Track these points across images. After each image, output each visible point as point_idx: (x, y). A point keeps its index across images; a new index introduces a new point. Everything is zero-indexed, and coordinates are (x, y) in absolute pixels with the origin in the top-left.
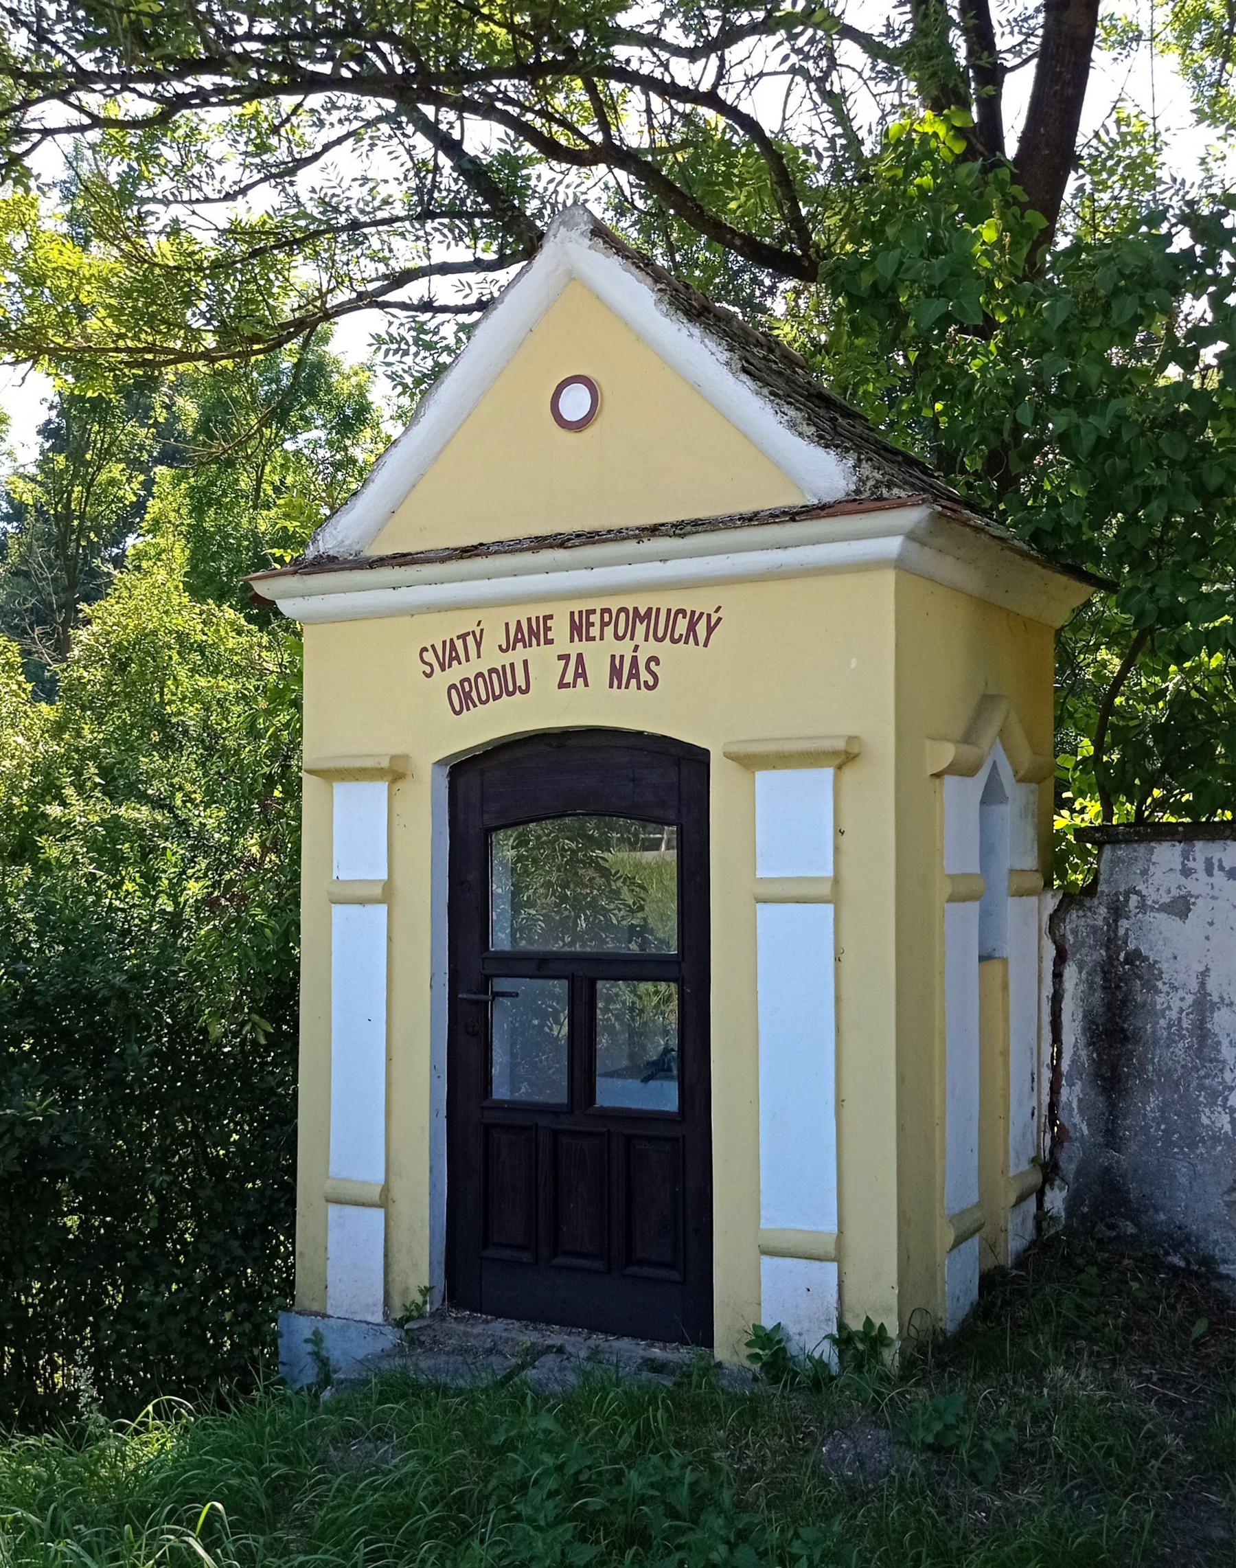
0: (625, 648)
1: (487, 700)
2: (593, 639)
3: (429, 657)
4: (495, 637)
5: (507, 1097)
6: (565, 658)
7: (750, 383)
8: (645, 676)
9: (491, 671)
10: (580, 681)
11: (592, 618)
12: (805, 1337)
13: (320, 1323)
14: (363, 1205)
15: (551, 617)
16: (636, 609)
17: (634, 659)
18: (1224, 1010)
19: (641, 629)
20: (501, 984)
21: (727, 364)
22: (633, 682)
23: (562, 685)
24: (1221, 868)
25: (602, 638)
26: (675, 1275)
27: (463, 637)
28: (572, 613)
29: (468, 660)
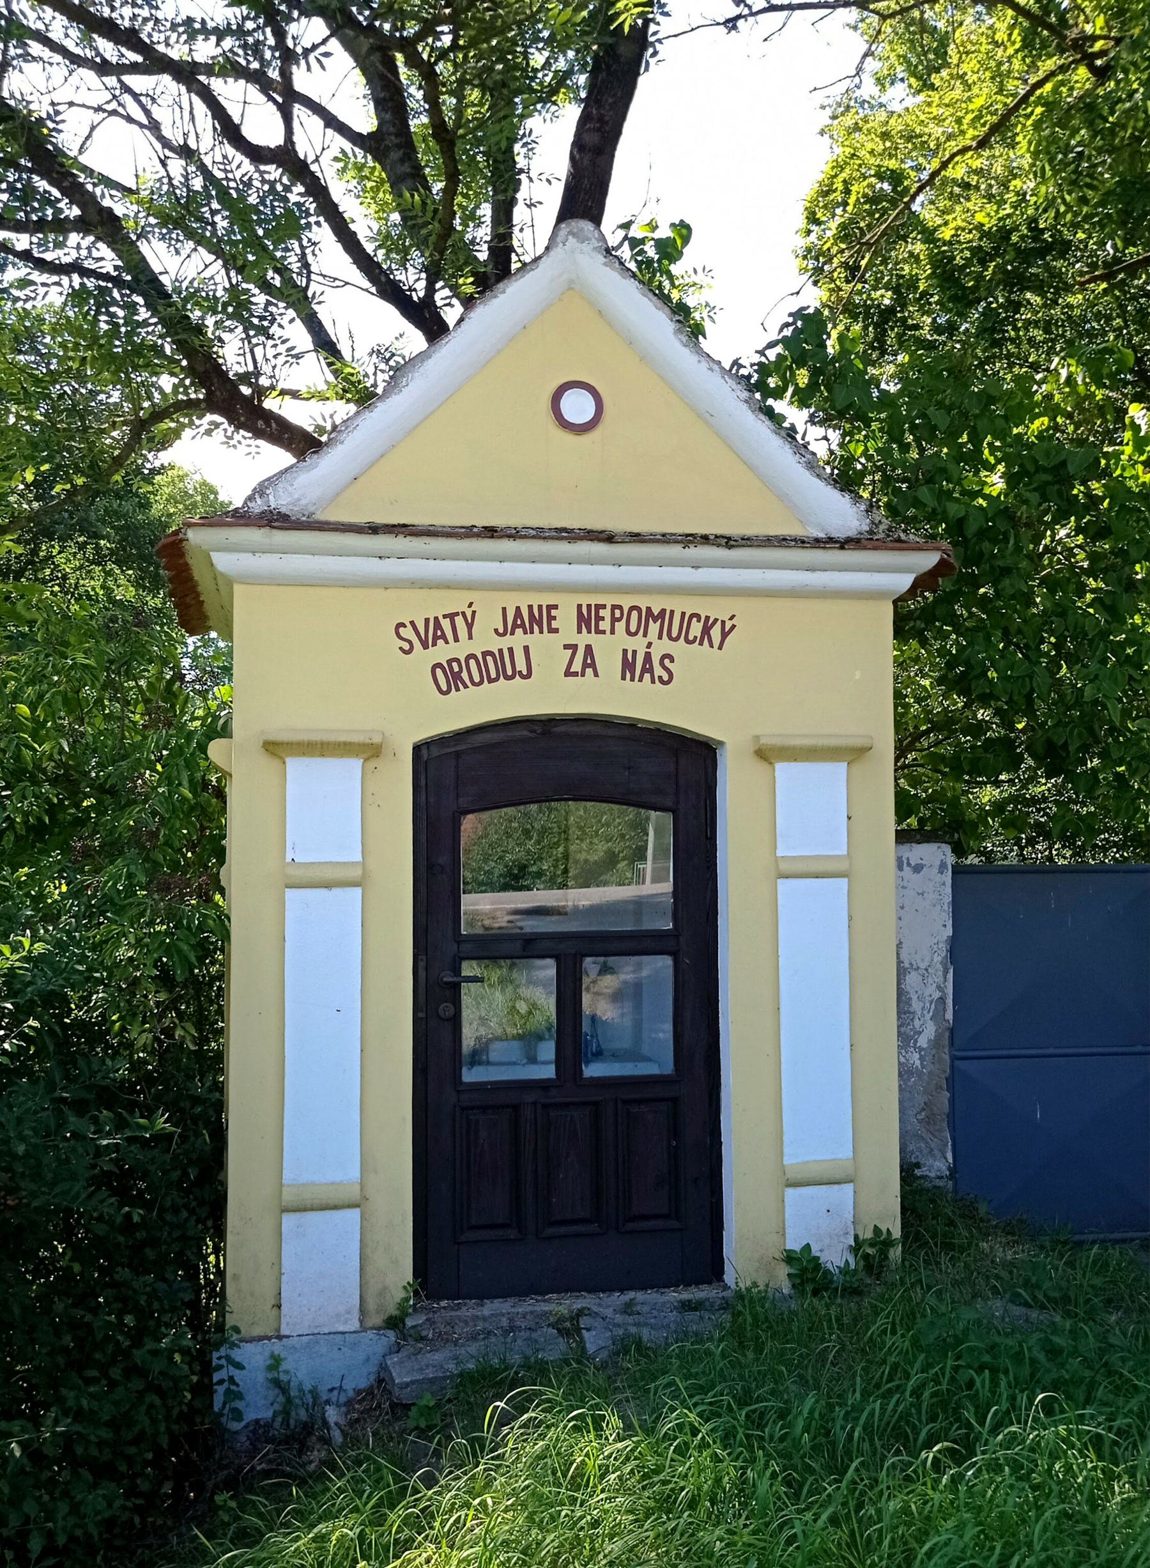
0: (638, 644)
1: (481, 682)
2: (604, 632)
3: (407, 632)
4: (488, 620)
5: (553, 1067)
6: (574, 648)
7: (768, 423)
8: (658, 671)
9: (485, 654)
10: (589, 671)
11: (602, 613)
12: (826, 1252)
13: (277, 1347)
14: (335, 1207)
15: (556, 607)
16: (649, 609)
17: (648, 657)
18: (913, 973)
19: (654, 628)
20: (469, 969)
21: (746, 401)
22: (647, 676)
23: (568, 673)
24: (909, 864)
25: (613, 632)
26: (674, 1224)
27: (451, 617)
28: (580, 606)
29: (456, 640)
